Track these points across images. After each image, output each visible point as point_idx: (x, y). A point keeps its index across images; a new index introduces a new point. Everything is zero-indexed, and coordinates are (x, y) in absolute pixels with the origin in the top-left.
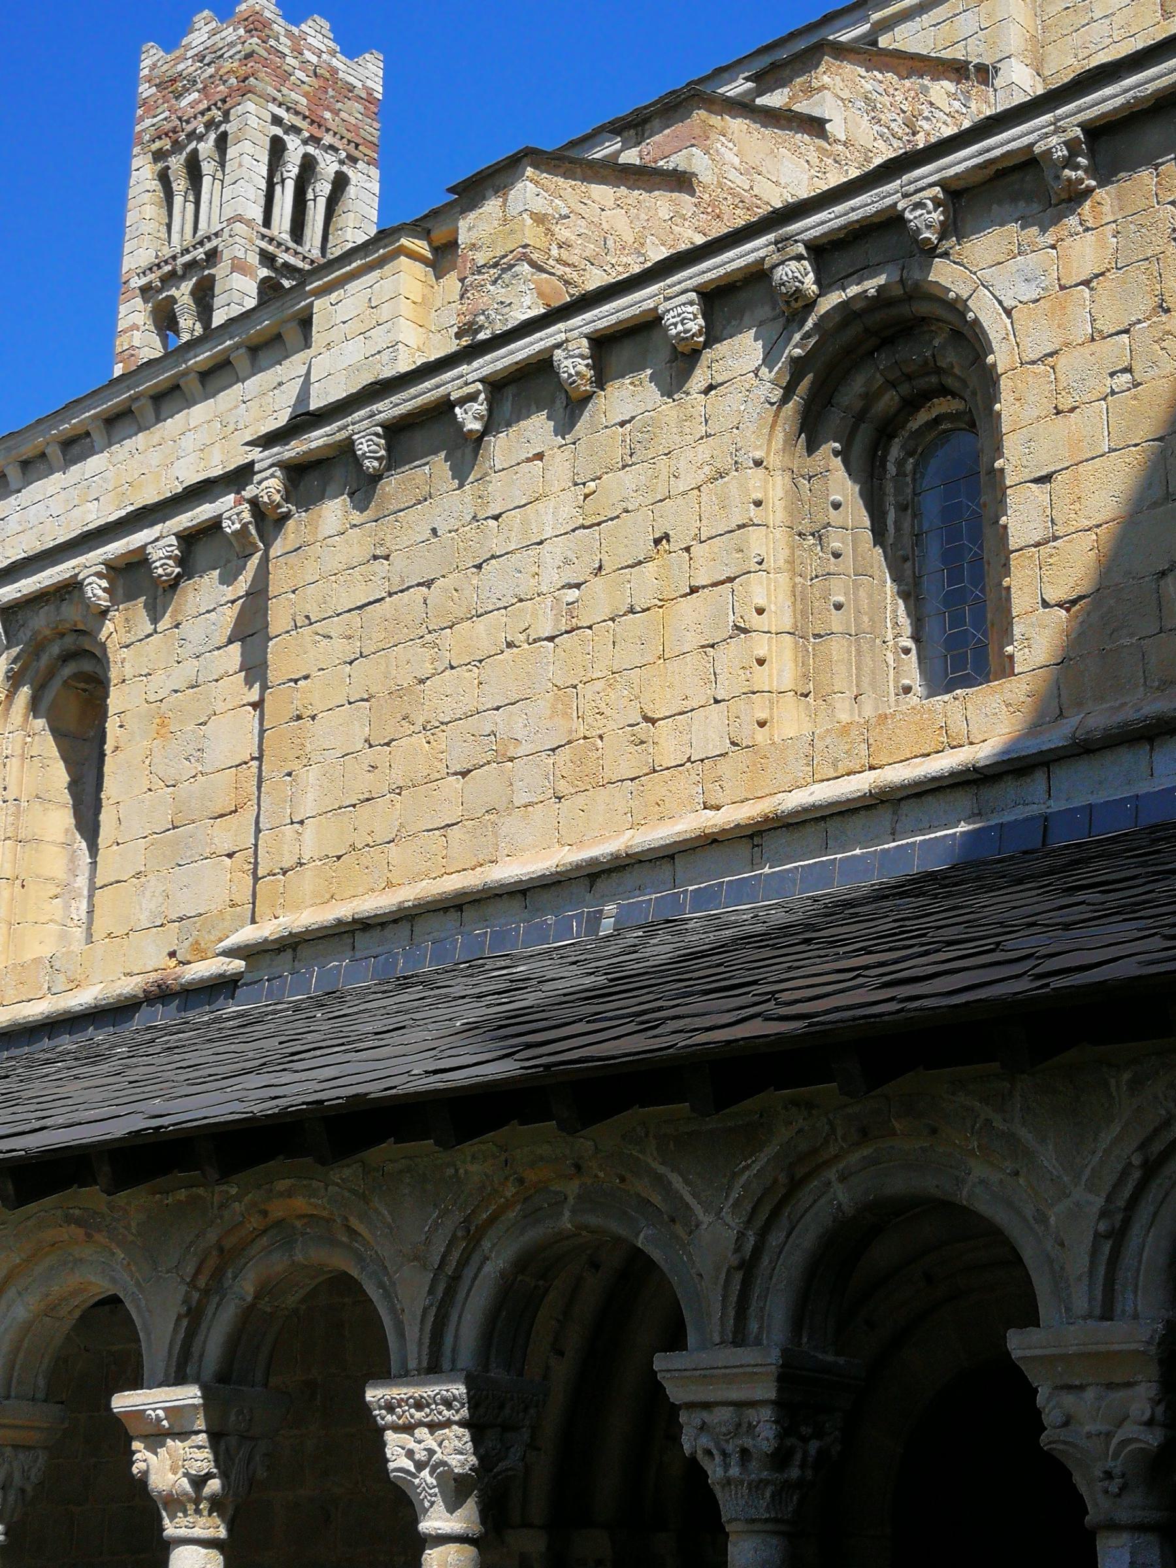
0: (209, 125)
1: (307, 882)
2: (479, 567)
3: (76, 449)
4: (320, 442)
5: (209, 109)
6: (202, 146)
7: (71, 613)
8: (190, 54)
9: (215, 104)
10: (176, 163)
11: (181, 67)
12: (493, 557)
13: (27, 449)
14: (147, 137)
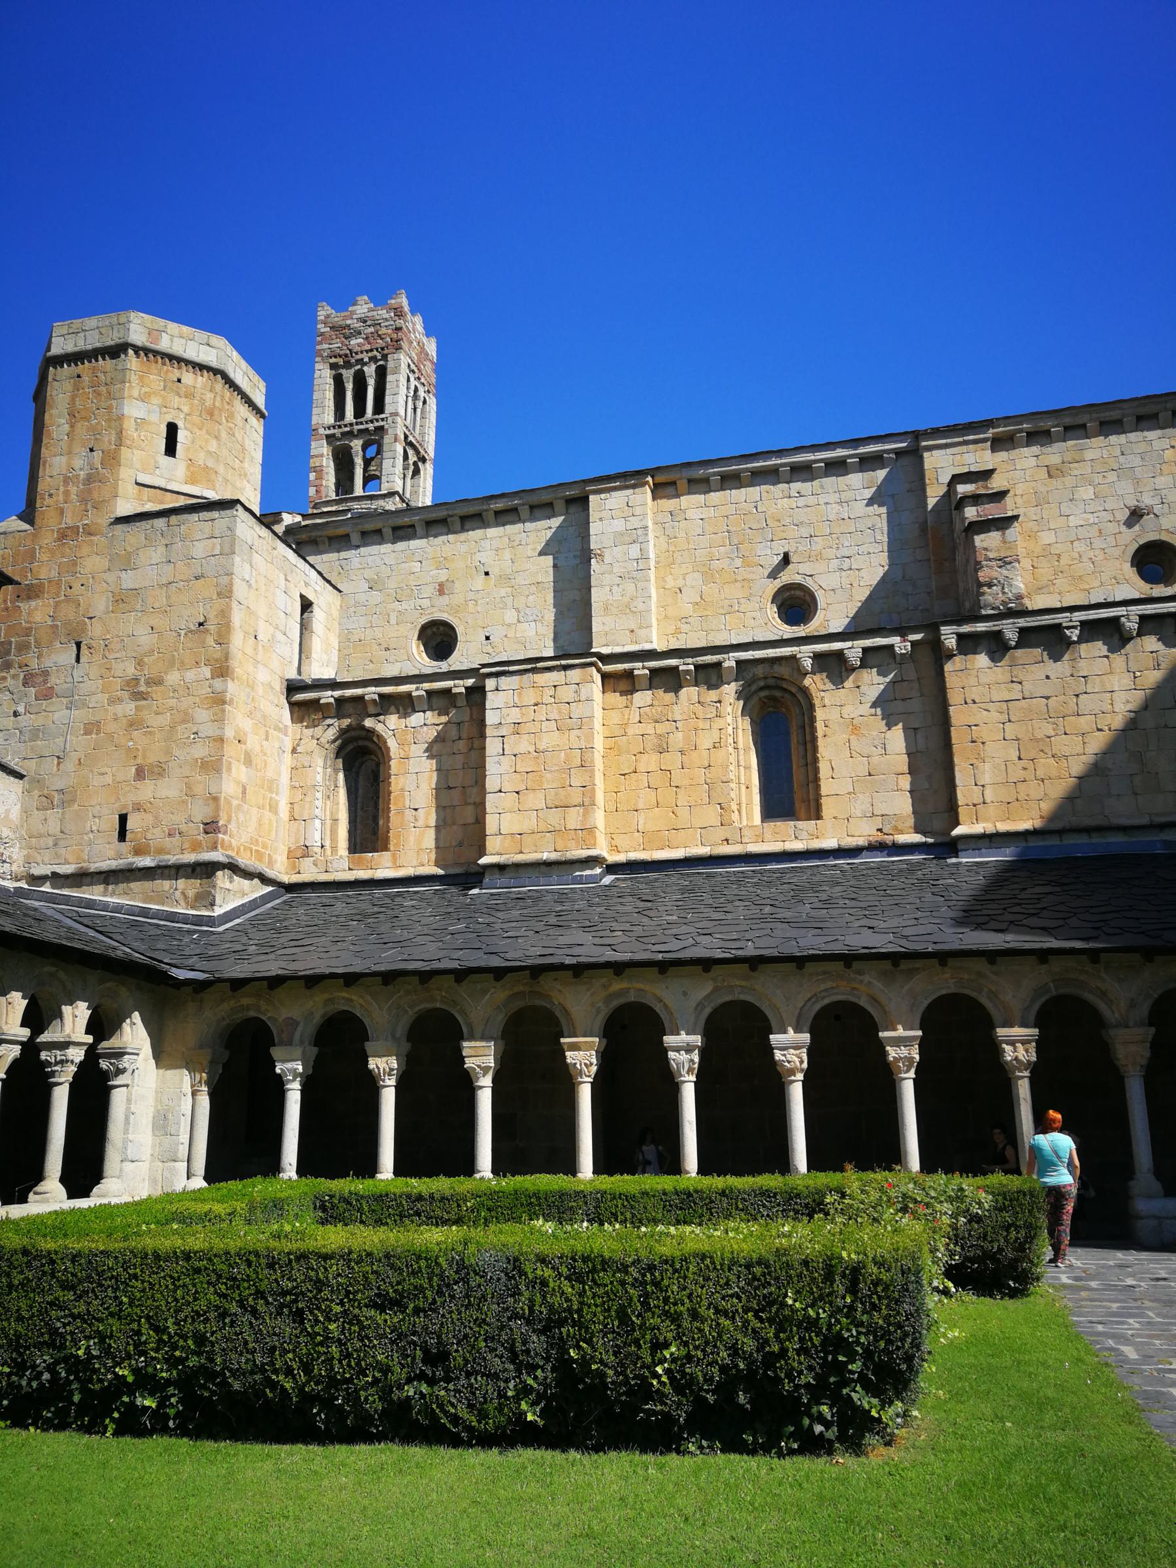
1: (991, 810)
2: (1077, 696)
3: (401, 533)
4: (984, 629)
5: (371, 350)
6: (365, 368)
7: (783, 671)
8: (355, 316)
9: (377, 349)
10: (348, 375)
11: (348, 322)
12: (1086, 693)
13: (369, 527)
14: (326, 354)
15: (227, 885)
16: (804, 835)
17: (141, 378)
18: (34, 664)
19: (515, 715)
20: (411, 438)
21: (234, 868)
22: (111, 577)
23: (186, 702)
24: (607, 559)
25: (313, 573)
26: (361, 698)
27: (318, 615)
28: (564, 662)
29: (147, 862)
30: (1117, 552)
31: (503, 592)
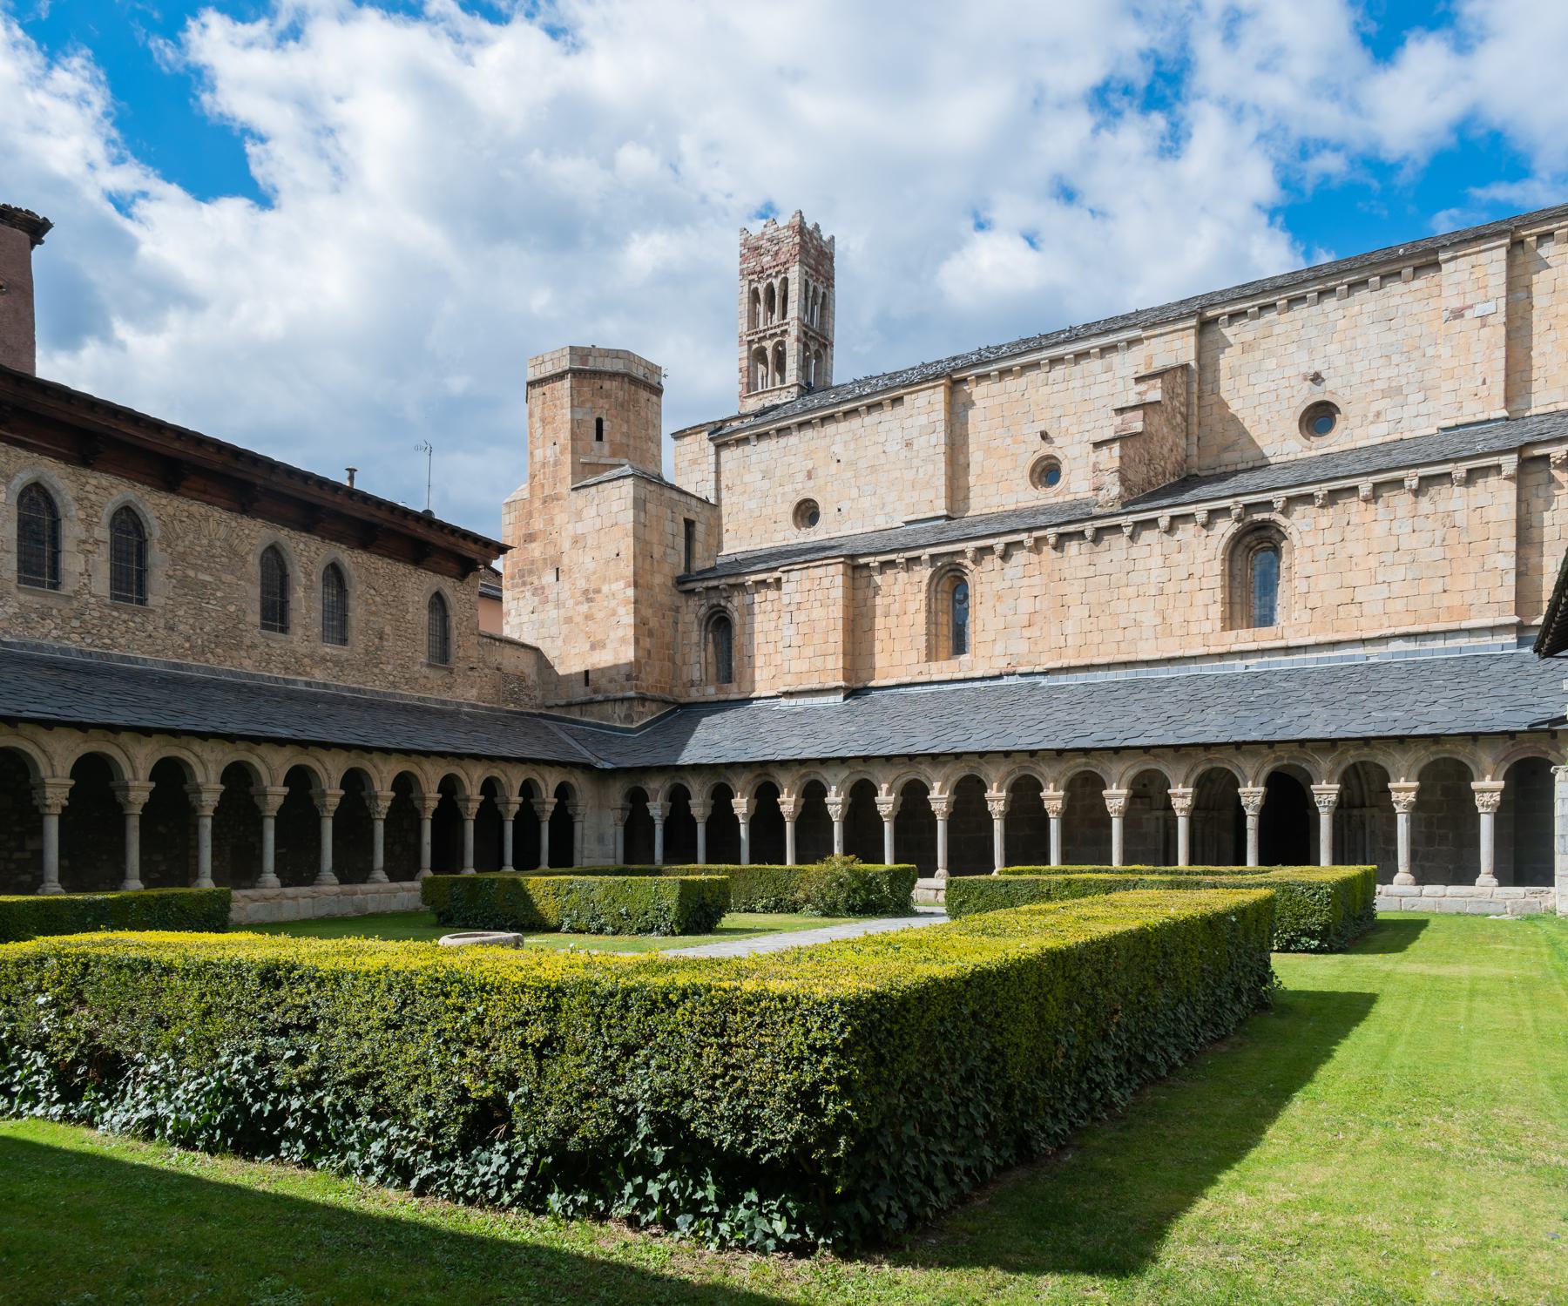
0: (778, 273)
1: (1070, 652)
6: (774, 281)
10: (761, 287)
15: (641, 709)
16: (965, 668)
17: (579, 392)
18: (536, 582)
19: (797, 598)
20: (811, 333)
21: (643, 699)
22: (570, 526)
23: (613, 603)
24: (915, 447)
25: (694, 502)
26: (716, 588)
27: (700, 529)
28: (825, 562)
29: (600, 697)
31: (849, 474)
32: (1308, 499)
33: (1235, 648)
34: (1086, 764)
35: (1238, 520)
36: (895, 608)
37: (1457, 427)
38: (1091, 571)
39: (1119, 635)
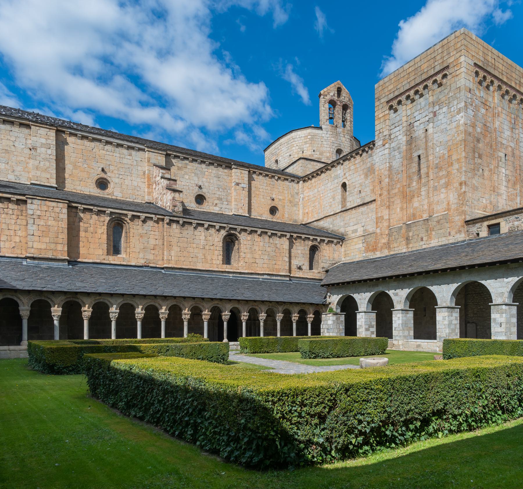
30: (192, 195)
32: (245, 231)
33: (227, 270)
34: (218, 304)
35: (227, 231)
36: (91, 229)
37: (238, 215)
38: (181, 235)
39: (190, 259)
